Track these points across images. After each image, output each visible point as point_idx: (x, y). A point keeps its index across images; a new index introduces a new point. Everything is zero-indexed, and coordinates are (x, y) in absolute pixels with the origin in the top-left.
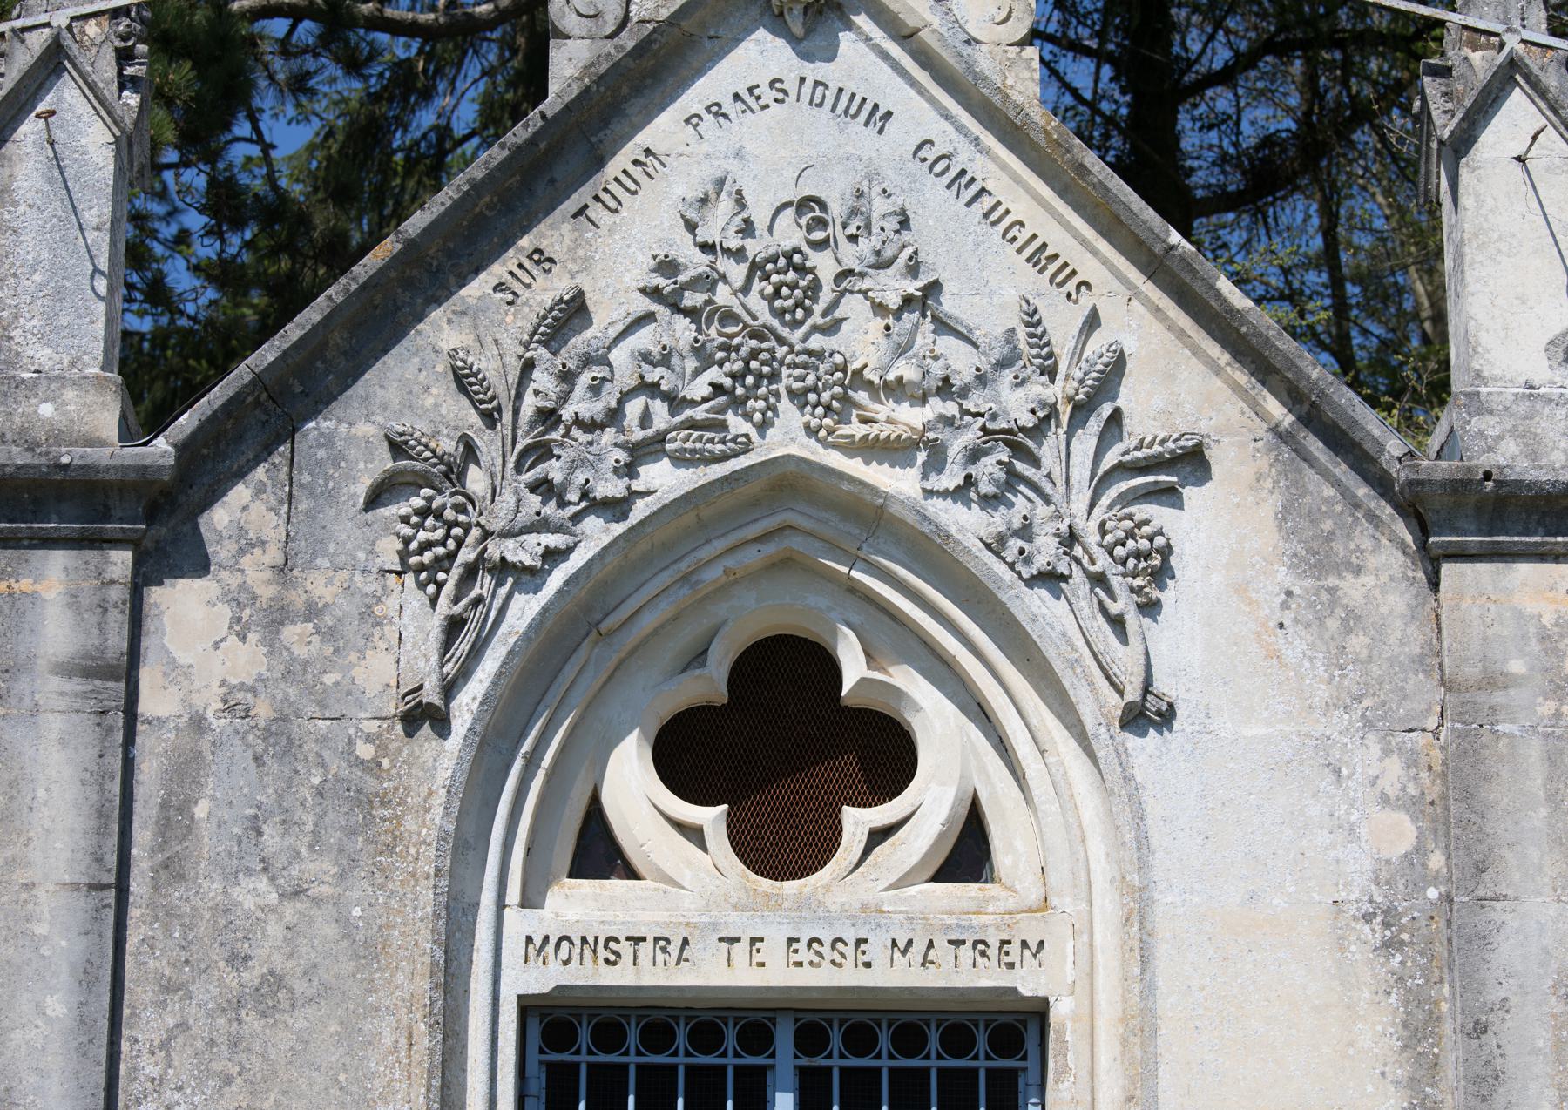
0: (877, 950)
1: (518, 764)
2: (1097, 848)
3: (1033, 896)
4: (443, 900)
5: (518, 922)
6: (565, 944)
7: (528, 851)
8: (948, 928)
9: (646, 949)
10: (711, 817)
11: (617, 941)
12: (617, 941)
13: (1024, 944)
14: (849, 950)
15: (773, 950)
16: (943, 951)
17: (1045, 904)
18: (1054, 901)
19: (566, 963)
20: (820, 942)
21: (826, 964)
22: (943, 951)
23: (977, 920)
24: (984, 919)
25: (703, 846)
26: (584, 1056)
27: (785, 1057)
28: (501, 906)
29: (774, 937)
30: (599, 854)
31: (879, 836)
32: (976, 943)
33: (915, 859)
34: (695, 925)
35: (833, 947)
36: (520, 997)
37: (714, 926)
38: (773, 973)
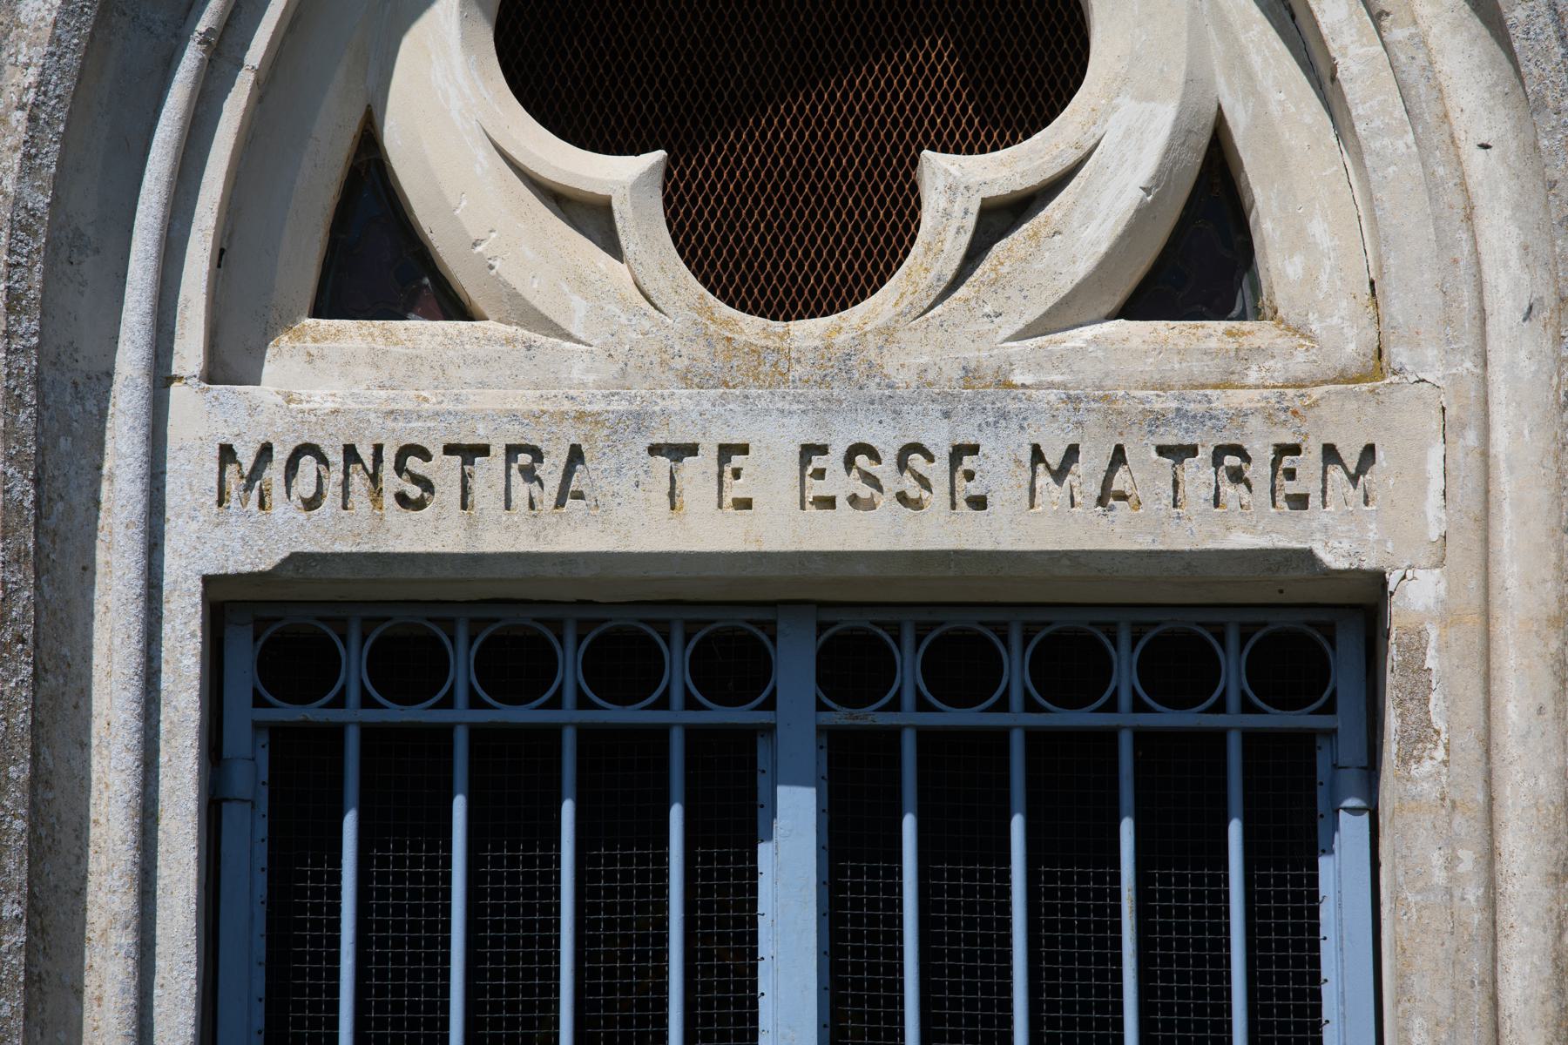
0: (999, 469)
1: (191, 57)
2: (1501, 234)
3: (1352, 345)
4: (28, 364)
5: (199, 418)
6: (308, 464)
7: (221, 257)
8: (1157, 420)
9: (489, 471)
10: (625, 177)
11: (425, 455)
12: (425, 455)
13: (1330, 454)
14: (937, 472)
15: (771, 475)
16: (1145, 473)
17: (1377, 364)
18: (1399, 355)
19: (311, 504)
20: (873, 454)
21: (886, 501)
22: (1145, 473)
23: (1222, 401)
24: (1239, 398)
25: (613, 246)
26: (353, 711)
27: (797, 708)
28: (161, 378)
29: (775, 439)
30: (381, 261)
31: (1002, 216)
32: (1220, 452)
33: (1083, 267)
34: (596, 419)
35: (902, 464)
36: (208, 581)
37: (639, 420)
38: (770, 520)
